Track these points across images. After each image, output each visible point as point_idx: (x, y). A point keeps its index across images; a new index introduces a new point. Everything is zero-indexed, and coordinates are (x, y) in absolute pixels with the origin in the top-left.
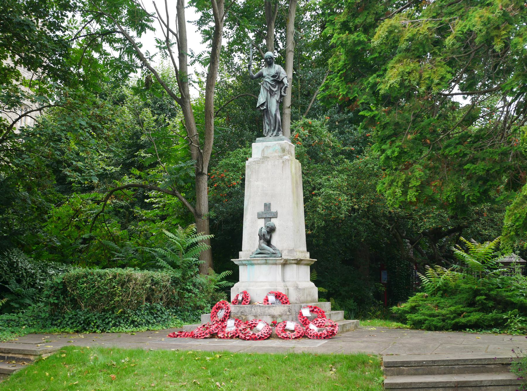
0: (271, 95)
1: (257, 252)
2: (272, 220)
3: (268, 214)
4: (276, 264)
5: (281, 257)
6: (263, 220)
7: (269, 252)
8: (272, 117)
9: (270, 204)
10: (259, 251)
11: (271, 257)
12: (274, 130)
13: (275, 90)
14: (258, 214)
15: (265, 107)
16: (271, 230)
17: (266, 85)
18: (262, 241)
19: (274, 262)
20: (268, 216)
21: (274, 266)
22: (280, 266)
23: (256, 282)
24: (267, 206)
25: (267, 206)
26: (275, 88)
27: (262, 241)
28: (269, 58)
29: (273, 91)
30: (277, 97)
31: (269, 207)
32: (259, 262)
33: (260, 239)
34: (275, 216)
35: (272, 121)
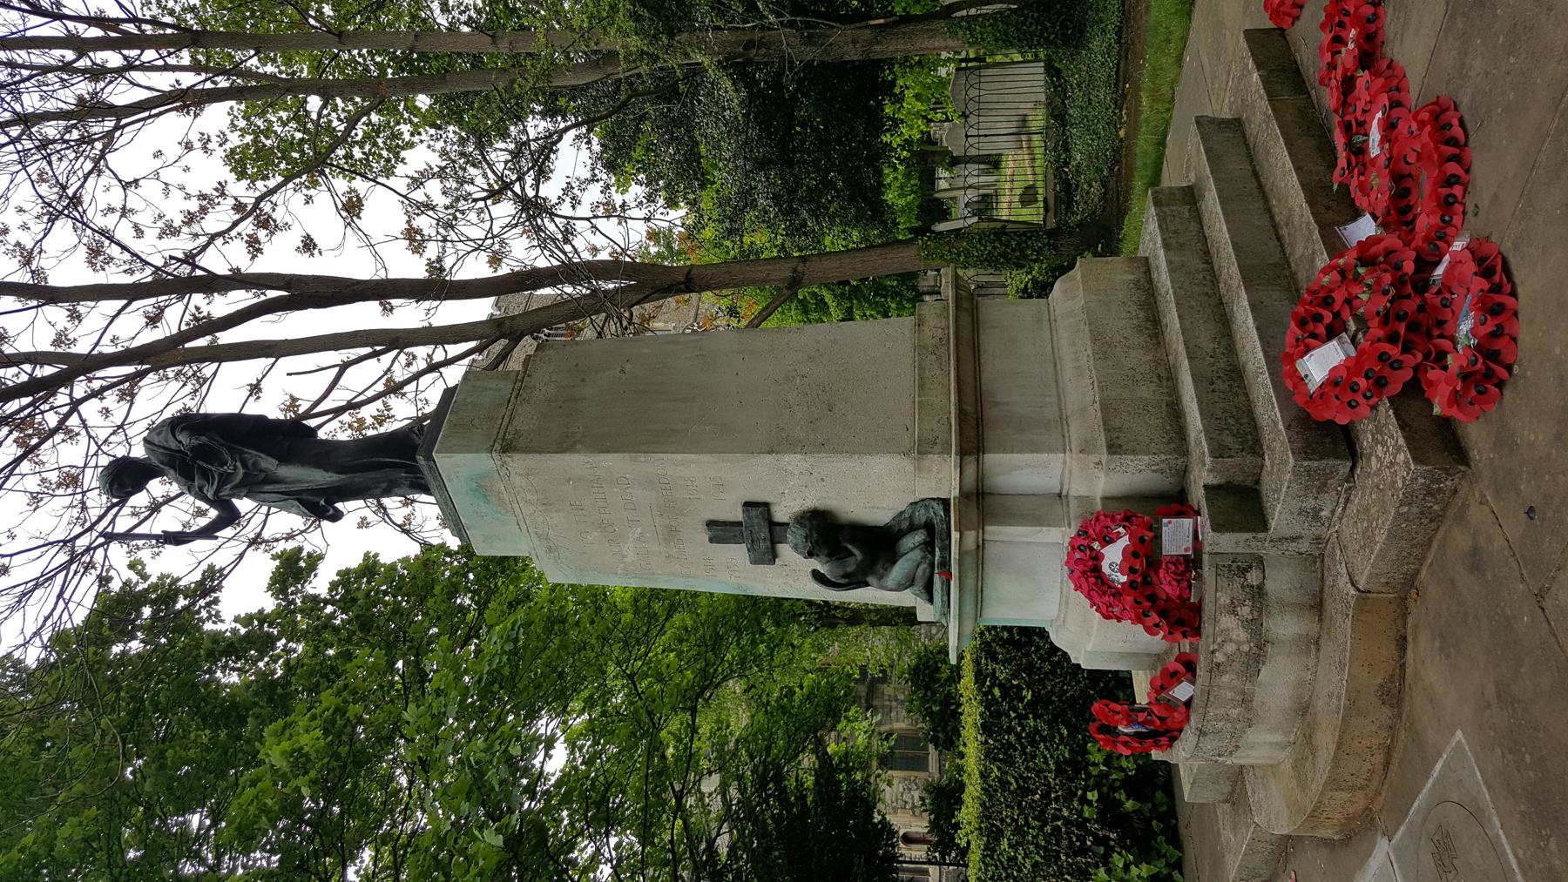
1: (925, 596)
2: (781, 514)
3: (758, 529)
4: (980, 547)
5: (945, 503)
6: (785, 550)
7: (924, 566)
11: (945, 563)
14: (755, 562)
18: (870, 579)
19: (970, 561)
20: (765, 533)
22: (992, 530)
24: (720, 531)
25: (720, 531)
27: (870, 579)
29: (245, 474)
30: (268, 463)
33: (867, 585)
34: (759, 508)
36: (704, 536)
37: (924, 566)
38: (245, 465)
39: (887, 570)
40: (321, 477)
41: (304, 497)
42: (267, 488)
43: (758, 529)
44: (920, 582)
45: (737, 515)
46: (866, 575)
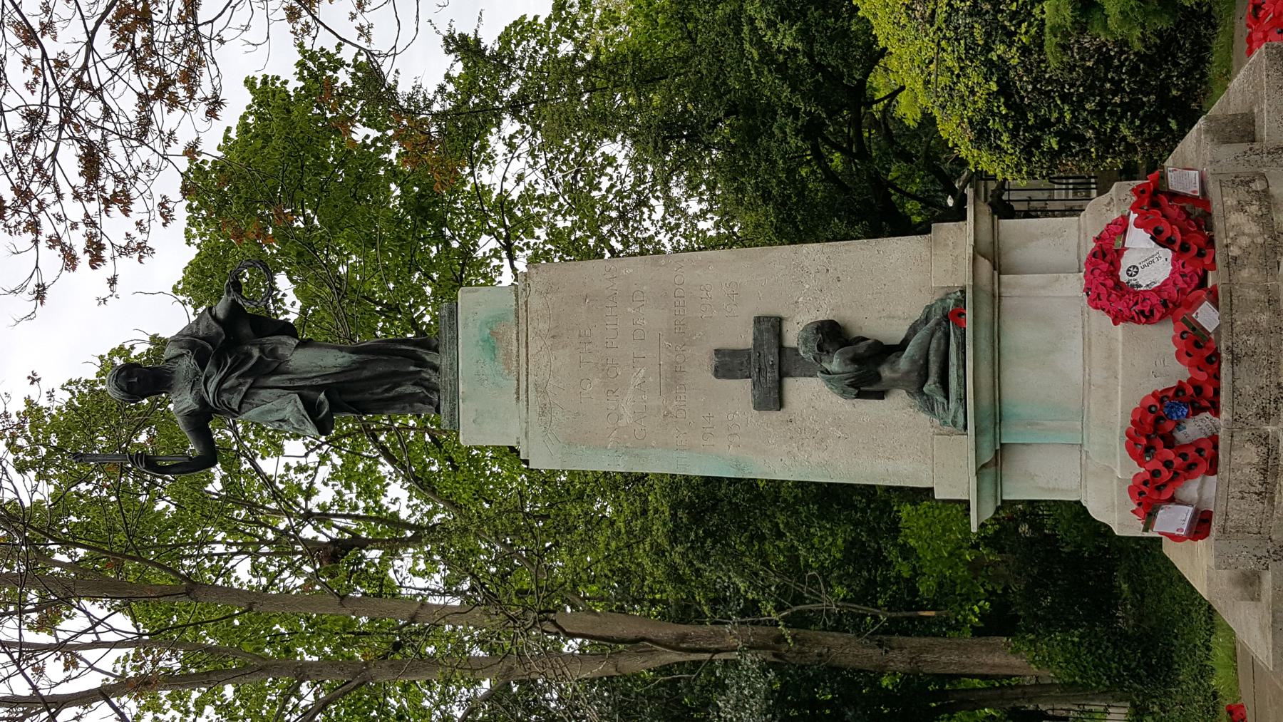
0: (276, 372)
7: (938, 334)
8: (362, 365)
9: (717, 352)
10: (931, 386)
12: (421, 363)
13: (256, 353)
15: (322, 396)
16: (831, 334)
17: (232, 389)
18: (886, 372)
21: (1006, 302)
23: (1087, 384)
24: (728, 364)
25: (728, 364)
26: (250, 356)
28: (129, 376)
29: (260, 358)
31: (734, 353)
32: (986, 381)
35: (381, 369)
36: (708, 362)
37: (938, 334)
38: (262, 350)
39: (899, 357)
40: (333, 360)
41: (305, 392)
42: (273, 380)
43: (765, 364)
44: (934, 369)
45: (743, 338)
46: (879, 365)
